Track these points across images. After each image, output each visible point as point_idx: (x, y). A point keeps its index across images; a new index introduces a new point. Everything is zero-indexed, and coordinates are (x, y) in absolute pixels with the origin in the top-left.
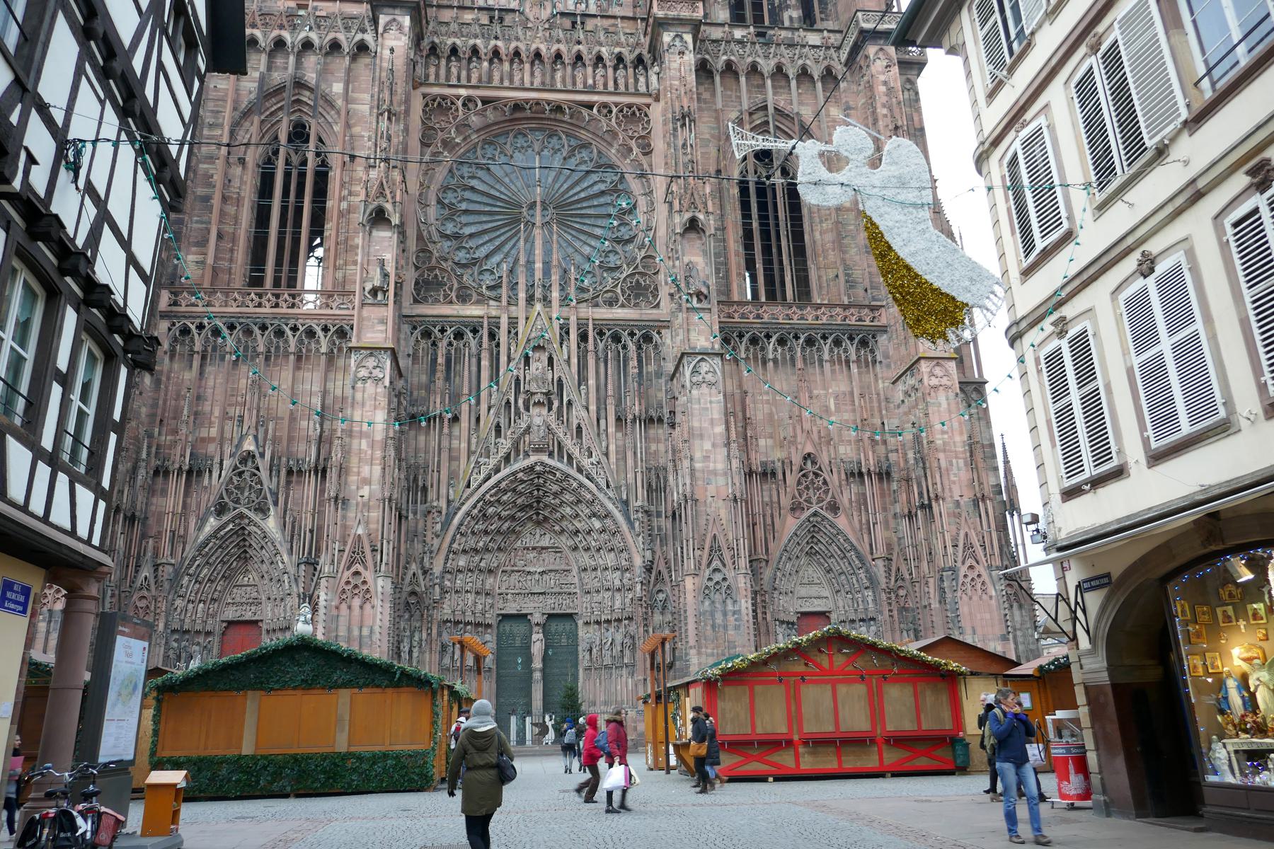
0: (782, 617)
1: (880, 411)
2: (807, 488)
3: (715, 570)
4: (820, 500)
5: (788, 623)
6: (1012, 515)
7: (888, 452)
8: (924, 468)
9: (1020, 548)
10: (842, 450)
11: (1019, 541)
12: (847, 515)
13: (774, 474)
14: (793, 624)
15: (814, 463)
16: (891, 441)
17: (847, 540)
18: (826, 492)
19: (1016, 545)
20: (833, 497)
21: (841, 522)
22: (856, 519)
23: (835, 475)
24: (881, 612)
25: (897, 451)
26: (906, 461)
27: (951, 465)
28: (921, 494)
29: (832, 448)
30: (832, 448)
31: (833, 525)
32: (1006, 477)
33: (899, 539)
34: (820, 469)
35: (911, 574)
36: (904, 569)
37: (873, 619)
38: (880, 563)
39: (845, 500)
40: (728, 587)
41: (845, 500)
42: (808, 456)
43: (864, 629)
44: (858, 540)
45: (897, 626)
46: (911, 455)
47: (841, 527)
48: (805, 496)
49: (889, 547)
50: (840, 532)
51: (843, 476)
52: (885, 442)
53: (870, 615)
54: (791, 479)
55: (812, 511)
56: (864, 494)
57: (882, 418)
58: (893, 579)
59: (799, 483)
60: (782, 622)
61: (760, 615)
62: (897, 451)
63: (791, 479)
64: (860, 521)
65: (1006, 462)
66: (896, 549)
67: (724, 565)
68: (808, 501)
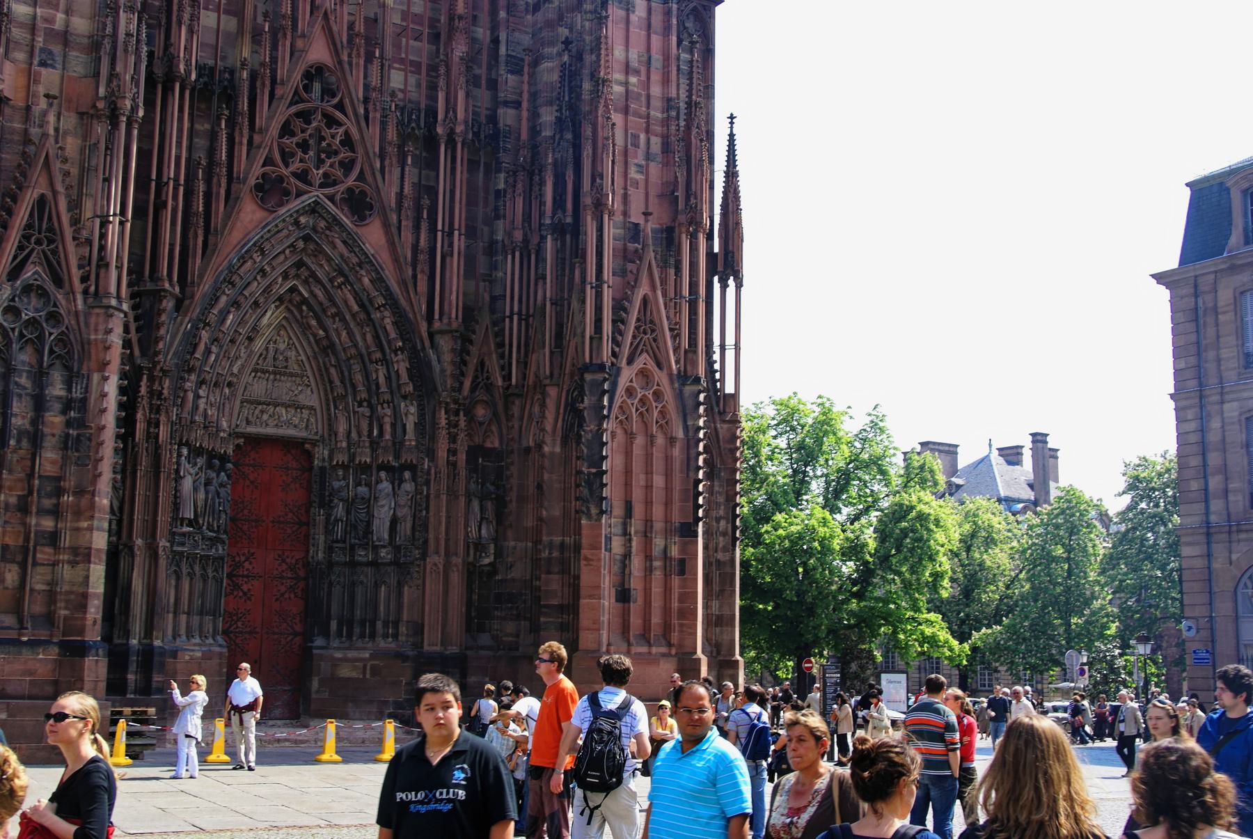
0: (199, 437)
1: (494, 13)
2: (304, 146)
3: (27, 289)
4: (328, 181)
5: (211, 455)
6: (724, 287)
7: (496, 103)
8: (577, 147)
9: (730, 355)
10: (396, 79)
11: (730, 340)
12: (386, 225)
13: (230, 97)
14: (224, 458)
15: (328, 92)
16: (509, 81)
17: (379, 281)
18: (347, 166)
19: (723, 347)
20: (361, 177)
21: (373, 236)
22: (407, 236)
23: (375, 130)
24: (431, 454)
25: (517, 105)
26: (534, 131)
27: (636, 145)
28: (559, 203)
29: (375, 69)
30: (375, 69)
31: (352, 243)
32: (725, 206)
33: (494, 299)
34: (340, 107)
35: (508, 377)
36: (493, 363)
37: (412, 468)
38: (445, 343)
39: (390, 193)
40: (62, 340)
41: (390, 193)
42: (315, 73)
43: (386, 486)
44: (403, 283)
45: (461, 487)
46: (548, 116)
47: (370, 250)
48: (296, 166)
49: (469, 314)
50: (366, 261)
51: (392, 134)
52: (493, 85)
53: (406, 457)
54: (271, 118)
55: (308, 199)
56: (432, 192)
57: (494, 28)
58: (467, 384)
59: (286, 130)
60: (196, 452)
61: (140, 427)
62: (517, 105)
63: (271, 118)
64: (415, 248)
65: (731, 174)
66: (486, 319)
67: (58, 282)
68: (303, 176)
